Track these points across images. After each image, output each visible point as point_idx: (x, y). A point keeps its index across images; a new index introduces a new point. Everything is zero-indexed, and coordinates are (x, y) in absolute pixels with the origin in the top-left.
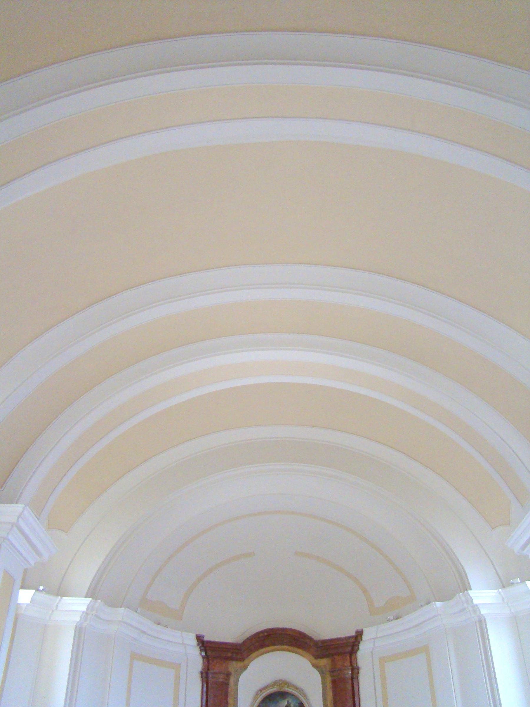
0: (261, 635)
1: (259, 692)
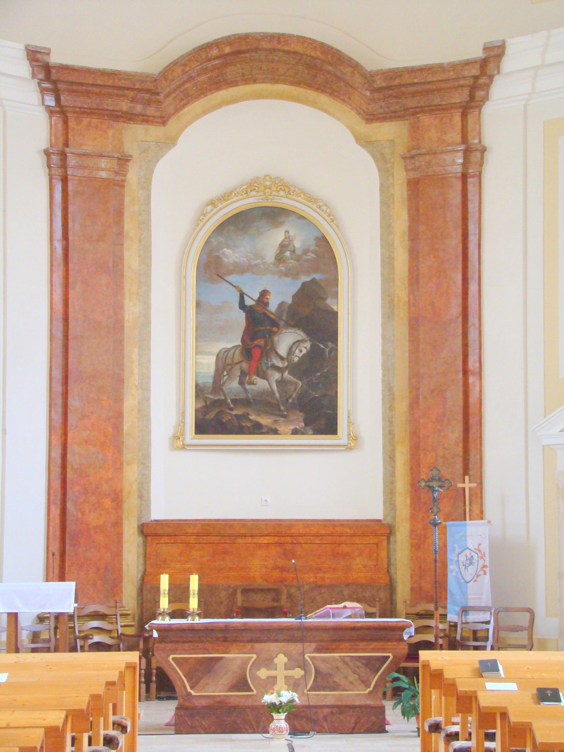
0: (215, 52)
1: (210, 207)
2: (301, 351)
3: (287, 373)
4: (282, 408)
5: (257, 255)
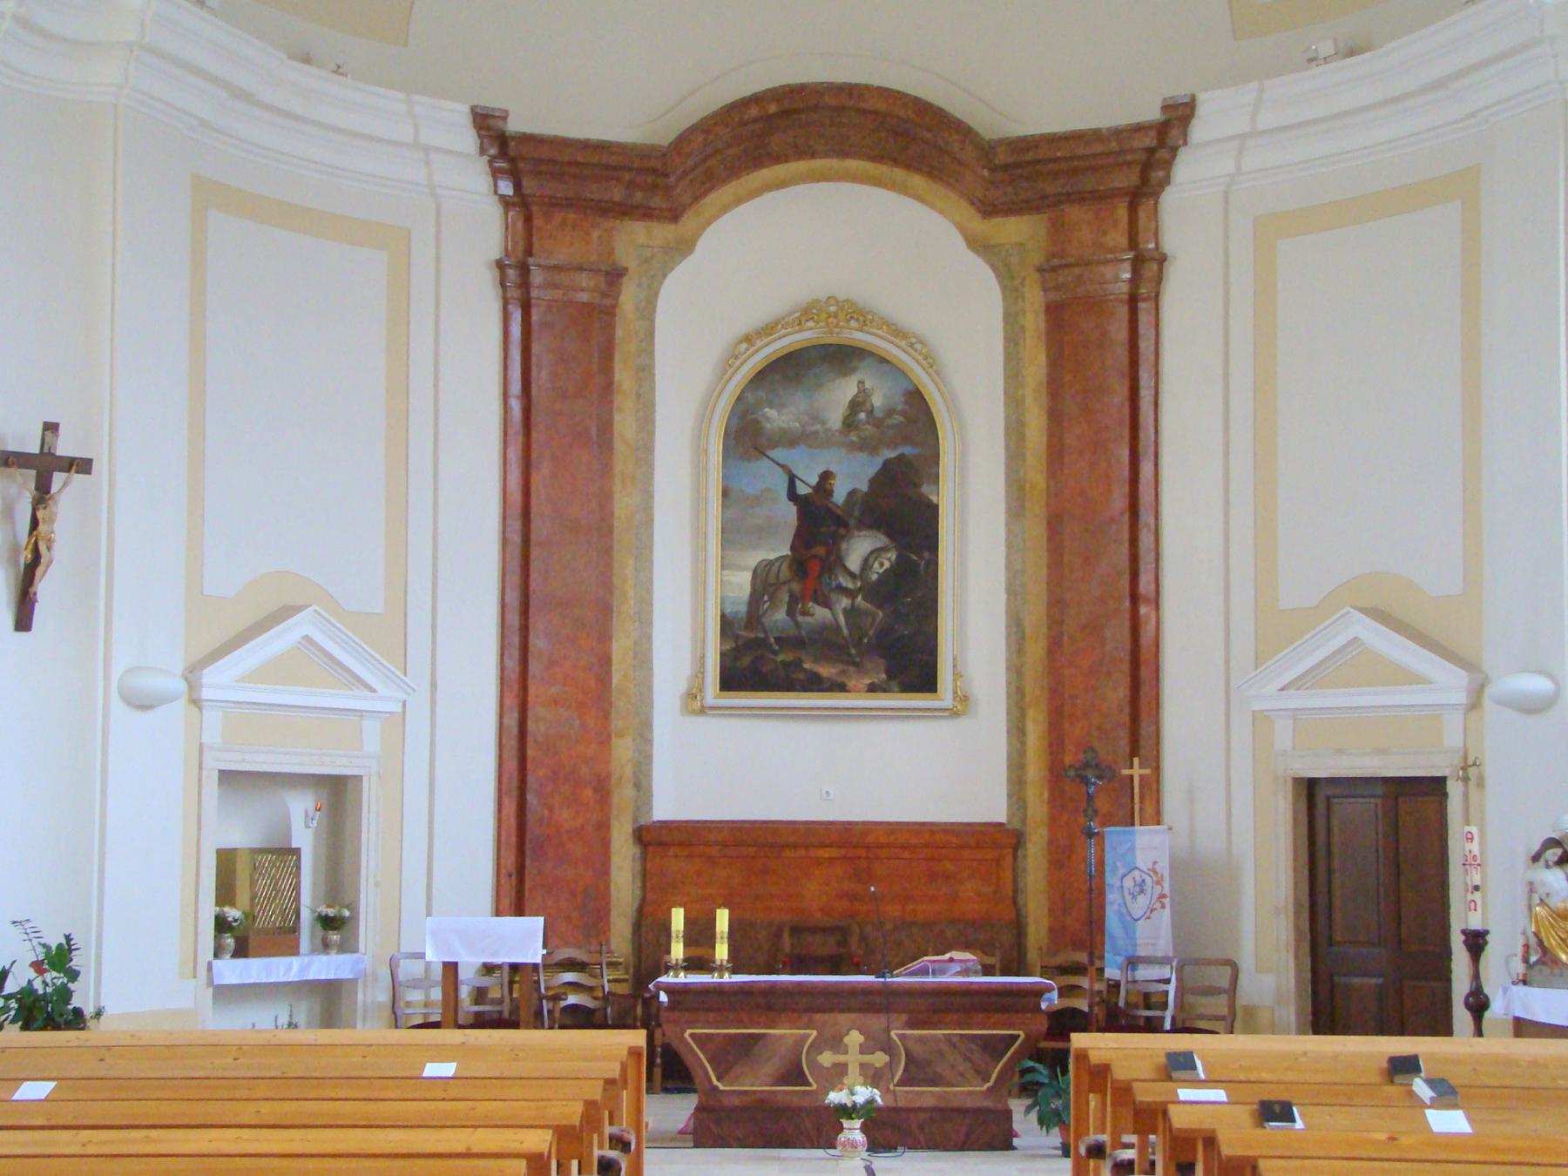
0: (754, 112)
1: (744, 346)
2: (882, 565)
3: (860, 597)
4: (853, 651)
5: (817, 418)
